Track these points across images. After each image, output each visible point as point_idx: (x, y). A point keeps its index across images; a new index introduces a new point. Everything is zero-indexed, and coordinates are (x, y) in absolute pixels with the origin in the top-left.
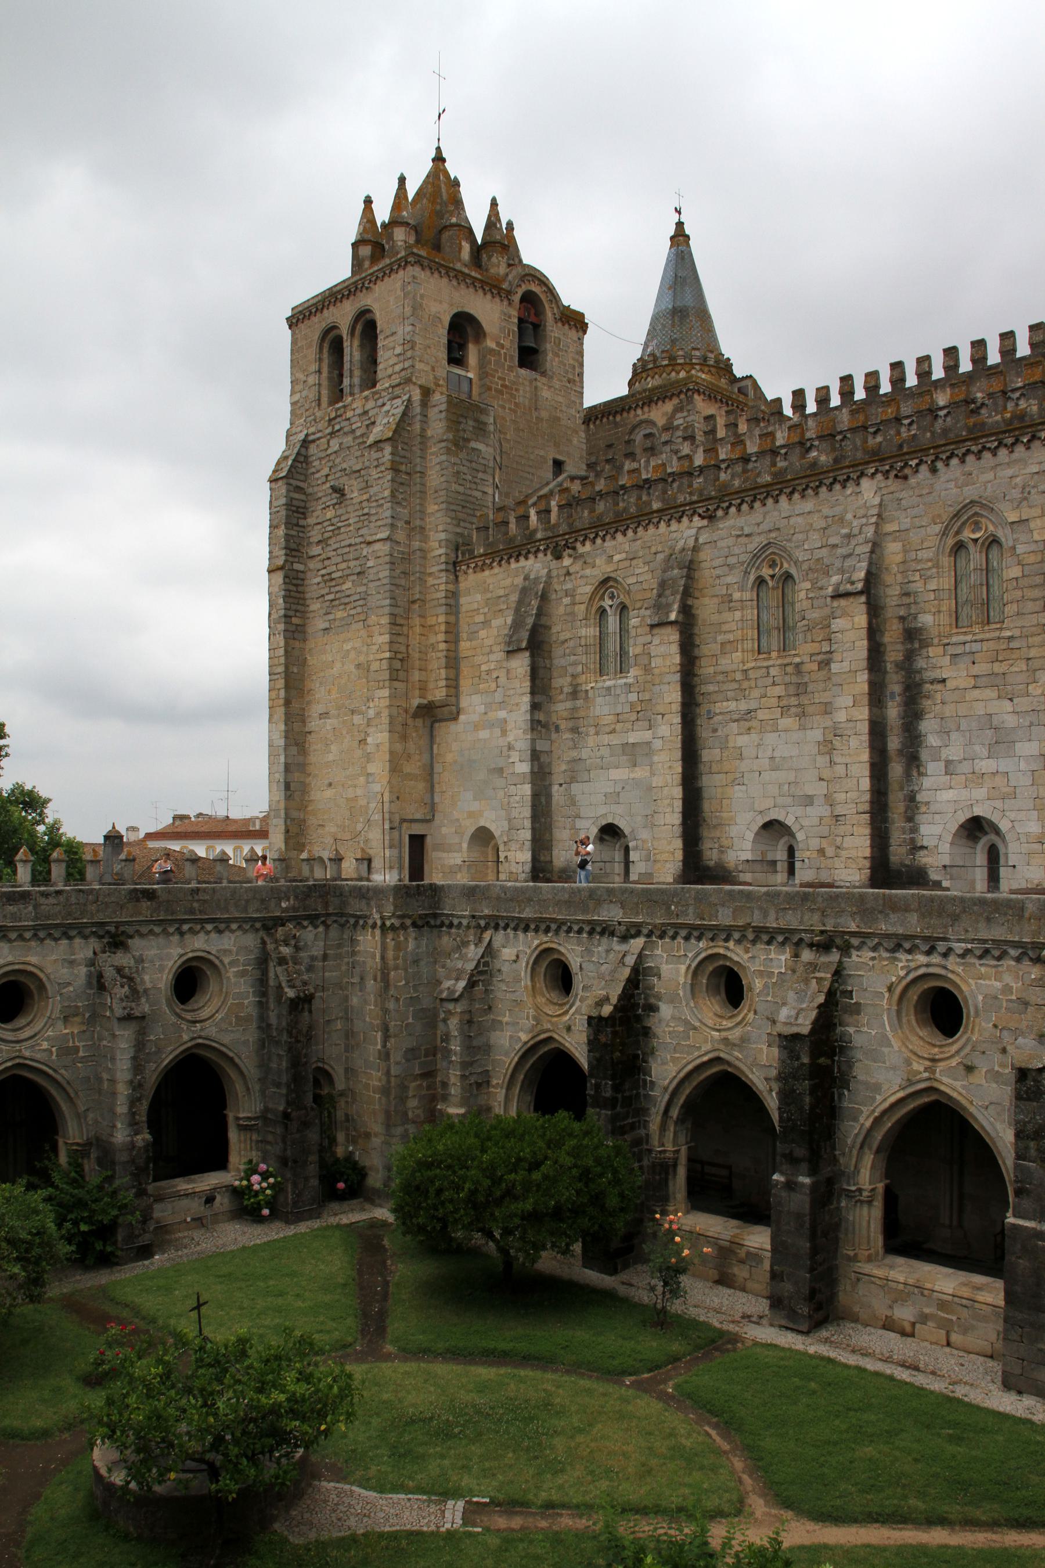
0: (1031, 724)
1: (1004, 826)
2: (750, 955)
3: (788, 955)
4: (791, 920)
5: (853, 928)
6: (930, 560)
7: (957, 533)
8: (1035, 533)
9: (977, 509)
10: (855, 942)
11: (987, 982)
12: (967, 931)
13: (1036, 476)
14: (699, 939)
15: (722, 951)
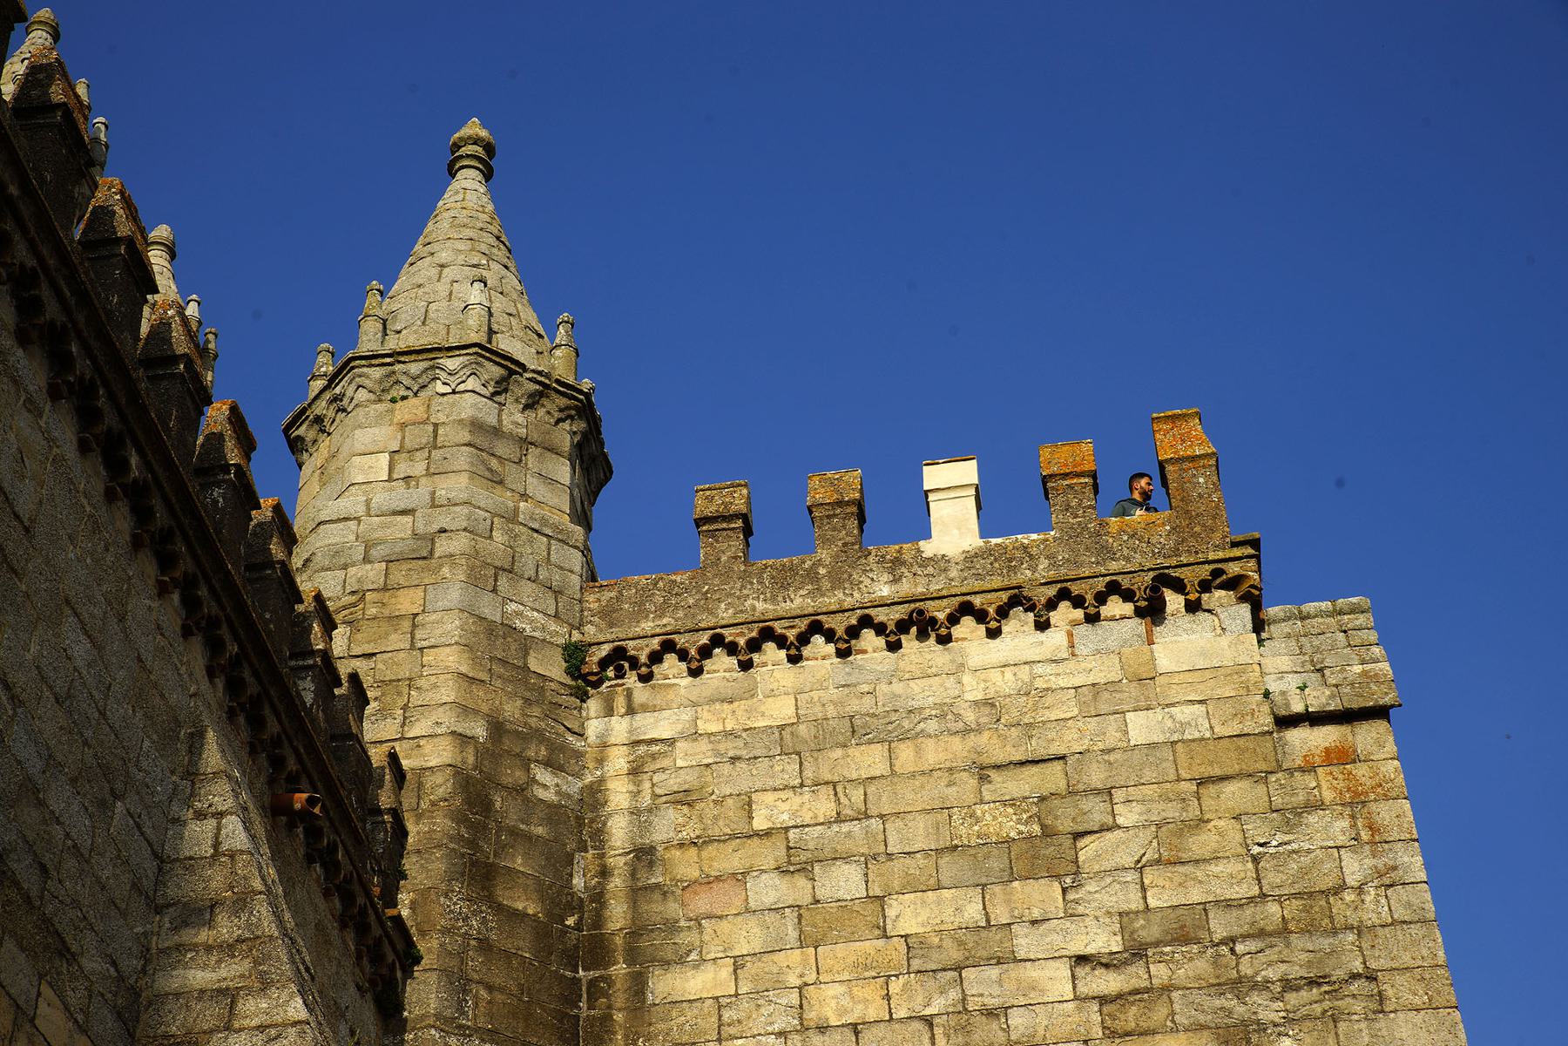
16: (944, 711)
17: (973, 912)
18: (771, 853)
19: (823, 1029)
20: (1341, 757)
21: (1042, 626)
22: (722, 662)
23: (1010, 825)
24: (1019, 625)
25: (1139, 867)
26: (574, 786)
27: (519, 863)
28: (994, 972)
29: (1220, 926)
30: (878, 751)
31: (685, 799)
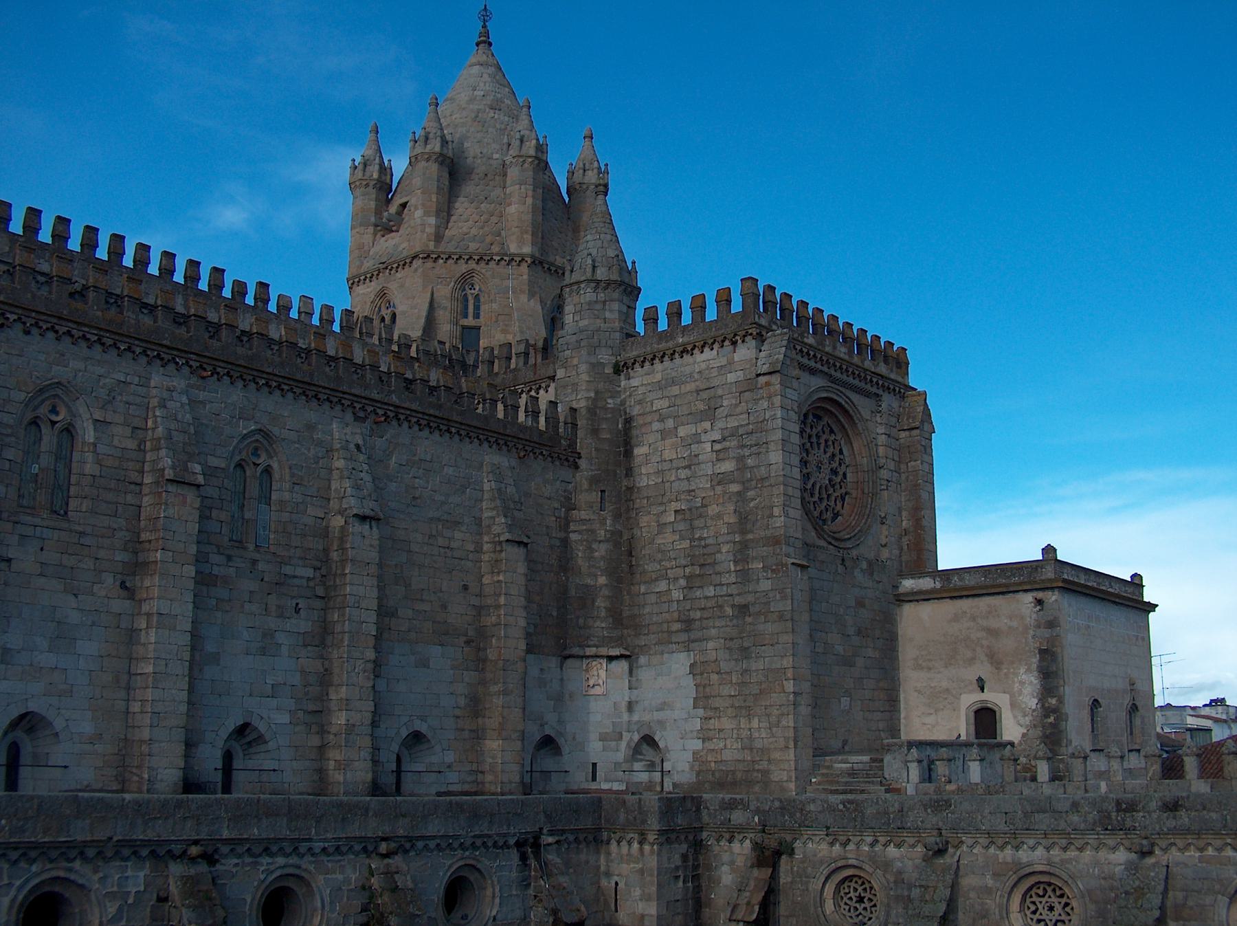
0: (93, 624)
1: (59, 724)
2: (101, 875)
3: (147, 871)
4: (159, 830)
5: (226, 834)
6: (11, 427)
7: (36, 408)
8: (116, 439)
9: (60, 392)
10: (225, 849)
11: (334, 876)
12: (327, 831)
13: (122, 385)
14: (33, 861)
15: (62, 874)
16: (691, 375)
17: (694, 431)
18: (656, 417)
19: (665, 461)
20: (768, 384)
21: (712, 349)
22: (647, 364)
23: (701, 406)
24: (706, 349)
25: (726, 417)
26: (618, 401)
27: (604, 426)
28: (697, 445)
29: (741, 431)
30: (678, 387)
31: (640, 402)
